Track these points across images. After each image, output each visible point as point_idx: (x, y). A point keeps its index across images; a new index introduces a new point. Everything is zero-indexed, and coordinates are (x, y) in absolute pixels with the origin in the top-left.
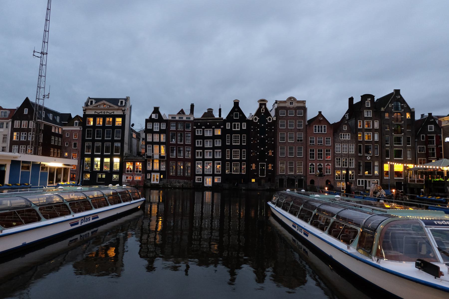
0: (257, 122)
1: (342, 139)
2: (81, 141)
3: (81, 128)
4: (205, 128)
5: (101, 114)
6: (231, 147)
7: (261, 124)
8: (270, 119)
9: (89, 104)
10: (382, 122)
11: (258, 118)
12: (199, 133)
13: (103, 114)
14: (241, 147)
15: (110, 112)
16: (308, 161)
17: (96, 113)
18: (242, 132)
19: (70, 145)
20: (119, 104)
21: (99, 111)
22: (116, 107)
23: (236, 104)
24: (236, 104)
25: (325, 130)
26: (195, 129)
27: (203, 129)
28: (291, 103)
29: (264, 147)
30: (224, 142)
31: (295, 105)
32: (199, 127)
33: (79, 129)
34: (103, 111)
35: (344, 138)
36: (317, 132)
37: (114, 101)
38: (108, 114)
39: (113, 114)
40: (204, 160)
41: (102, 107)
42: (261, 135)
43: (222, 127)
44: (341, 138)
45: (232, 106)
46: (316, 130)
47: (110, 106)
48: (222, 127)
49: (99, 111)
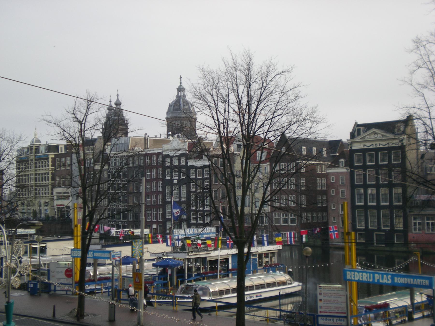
2: (349, 188)
3: (348, 169)
5: (371, 147)
9: (356, 134)
13: (374, 147)
15: (384, 143)
17: (365, 147)
19: (337, 193)
20: (396, 130)
21: (368, 144)
22: (390, 136)
33: (344, 170)
34: (374, 143)
37: (388, 127)
38: (381, 146)
39: (387, 146)
41: (372, 137)
47: (383, 135)
49: (368, 144)
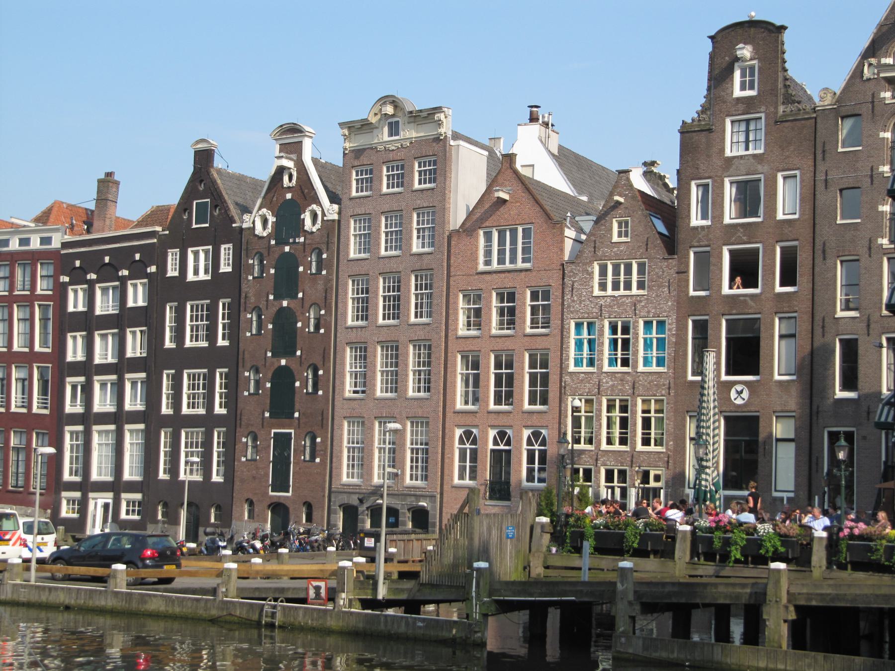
0: (269, 236)
1: (610, 291)
4: (99, 281)
6: (183, 358)
7: (281, 242)
8: (314, 216)
10: (821, 177)
11: (271, 219)
12: (76, 302)
14: (207, 358)
16: (449, 415)
18: (219, 286)
23: (204, 158)
24: (204, 158)
25: (526, 250)
26: (65, 286)
27: (91, 284)
28: (394, 129)
29: (289, 352)
30: (154, 338)
31: (409, 133)
32: (78, 277)
35: (616, 287)
36: (495, 265)
40: (88, 419)
42: (279, 297)
43: (153, 269)
44: (603, 286)
45: (192, 170)
46: (488, 253)
48: (153, 269)
